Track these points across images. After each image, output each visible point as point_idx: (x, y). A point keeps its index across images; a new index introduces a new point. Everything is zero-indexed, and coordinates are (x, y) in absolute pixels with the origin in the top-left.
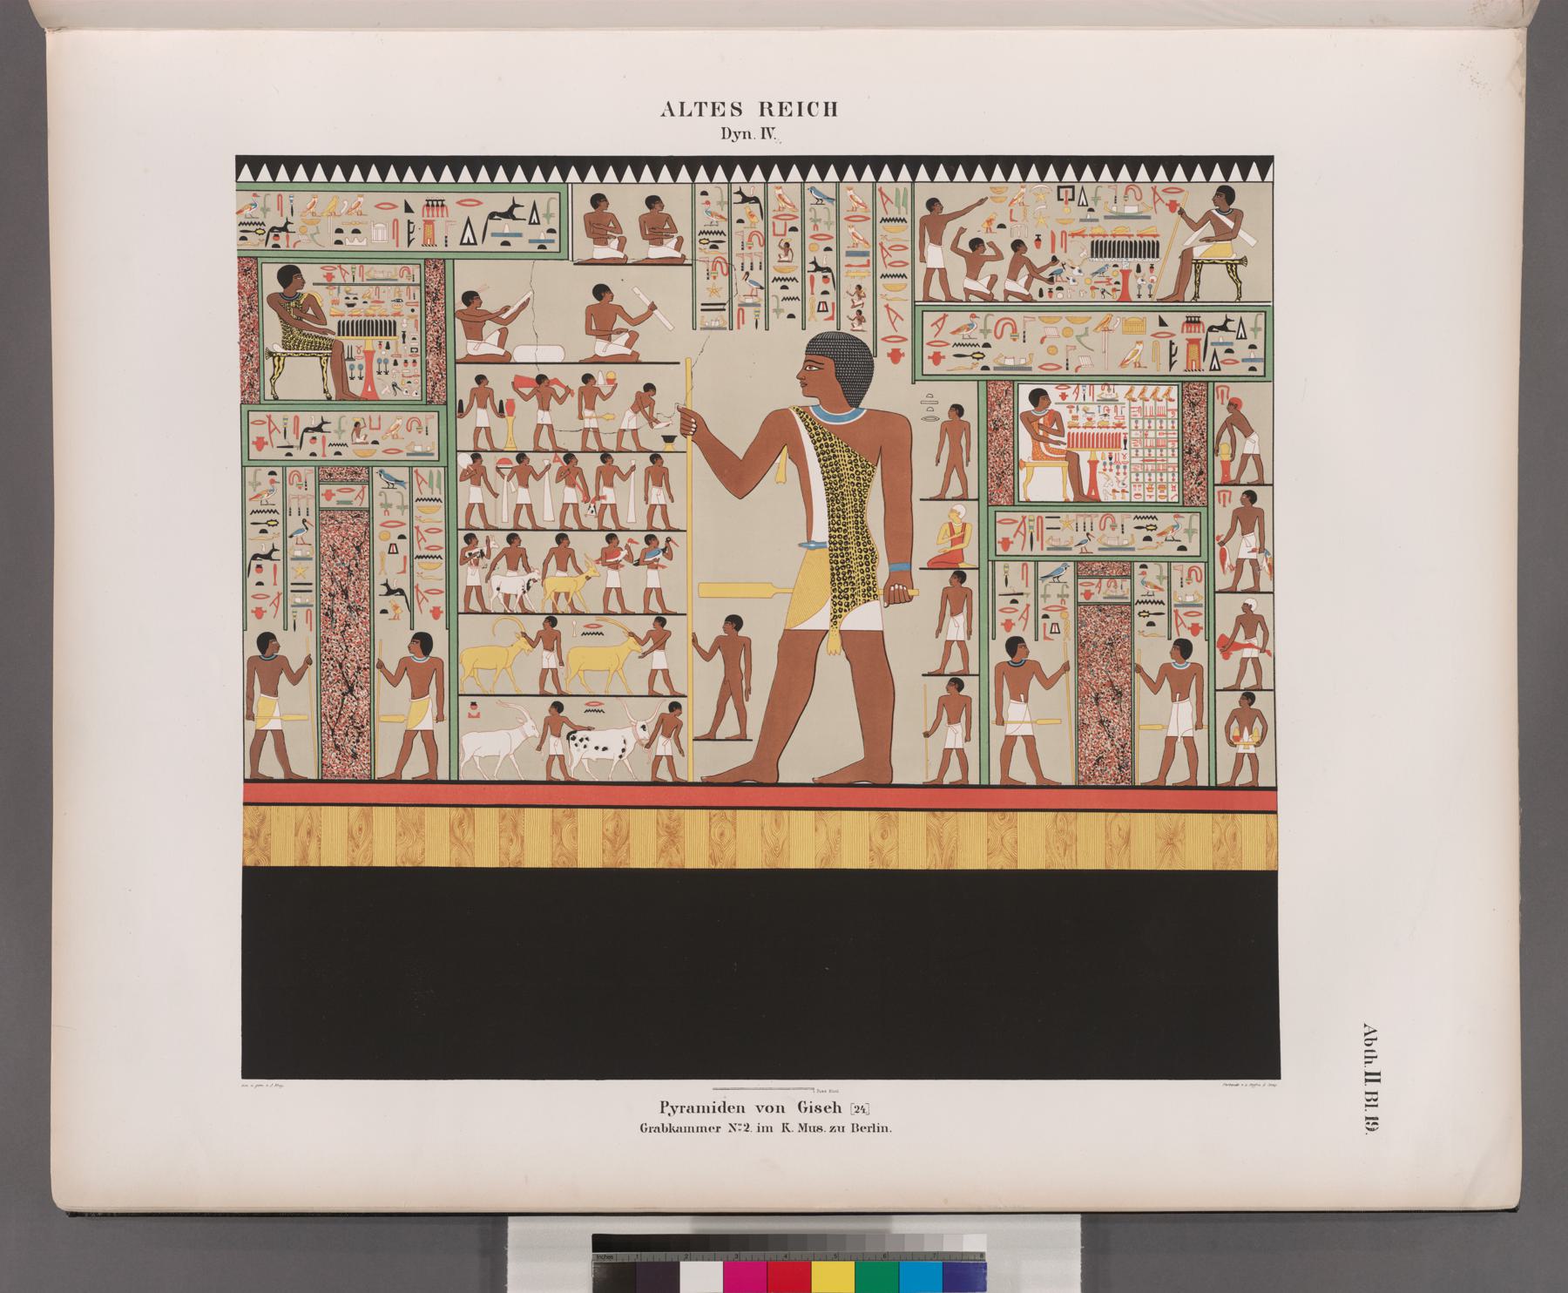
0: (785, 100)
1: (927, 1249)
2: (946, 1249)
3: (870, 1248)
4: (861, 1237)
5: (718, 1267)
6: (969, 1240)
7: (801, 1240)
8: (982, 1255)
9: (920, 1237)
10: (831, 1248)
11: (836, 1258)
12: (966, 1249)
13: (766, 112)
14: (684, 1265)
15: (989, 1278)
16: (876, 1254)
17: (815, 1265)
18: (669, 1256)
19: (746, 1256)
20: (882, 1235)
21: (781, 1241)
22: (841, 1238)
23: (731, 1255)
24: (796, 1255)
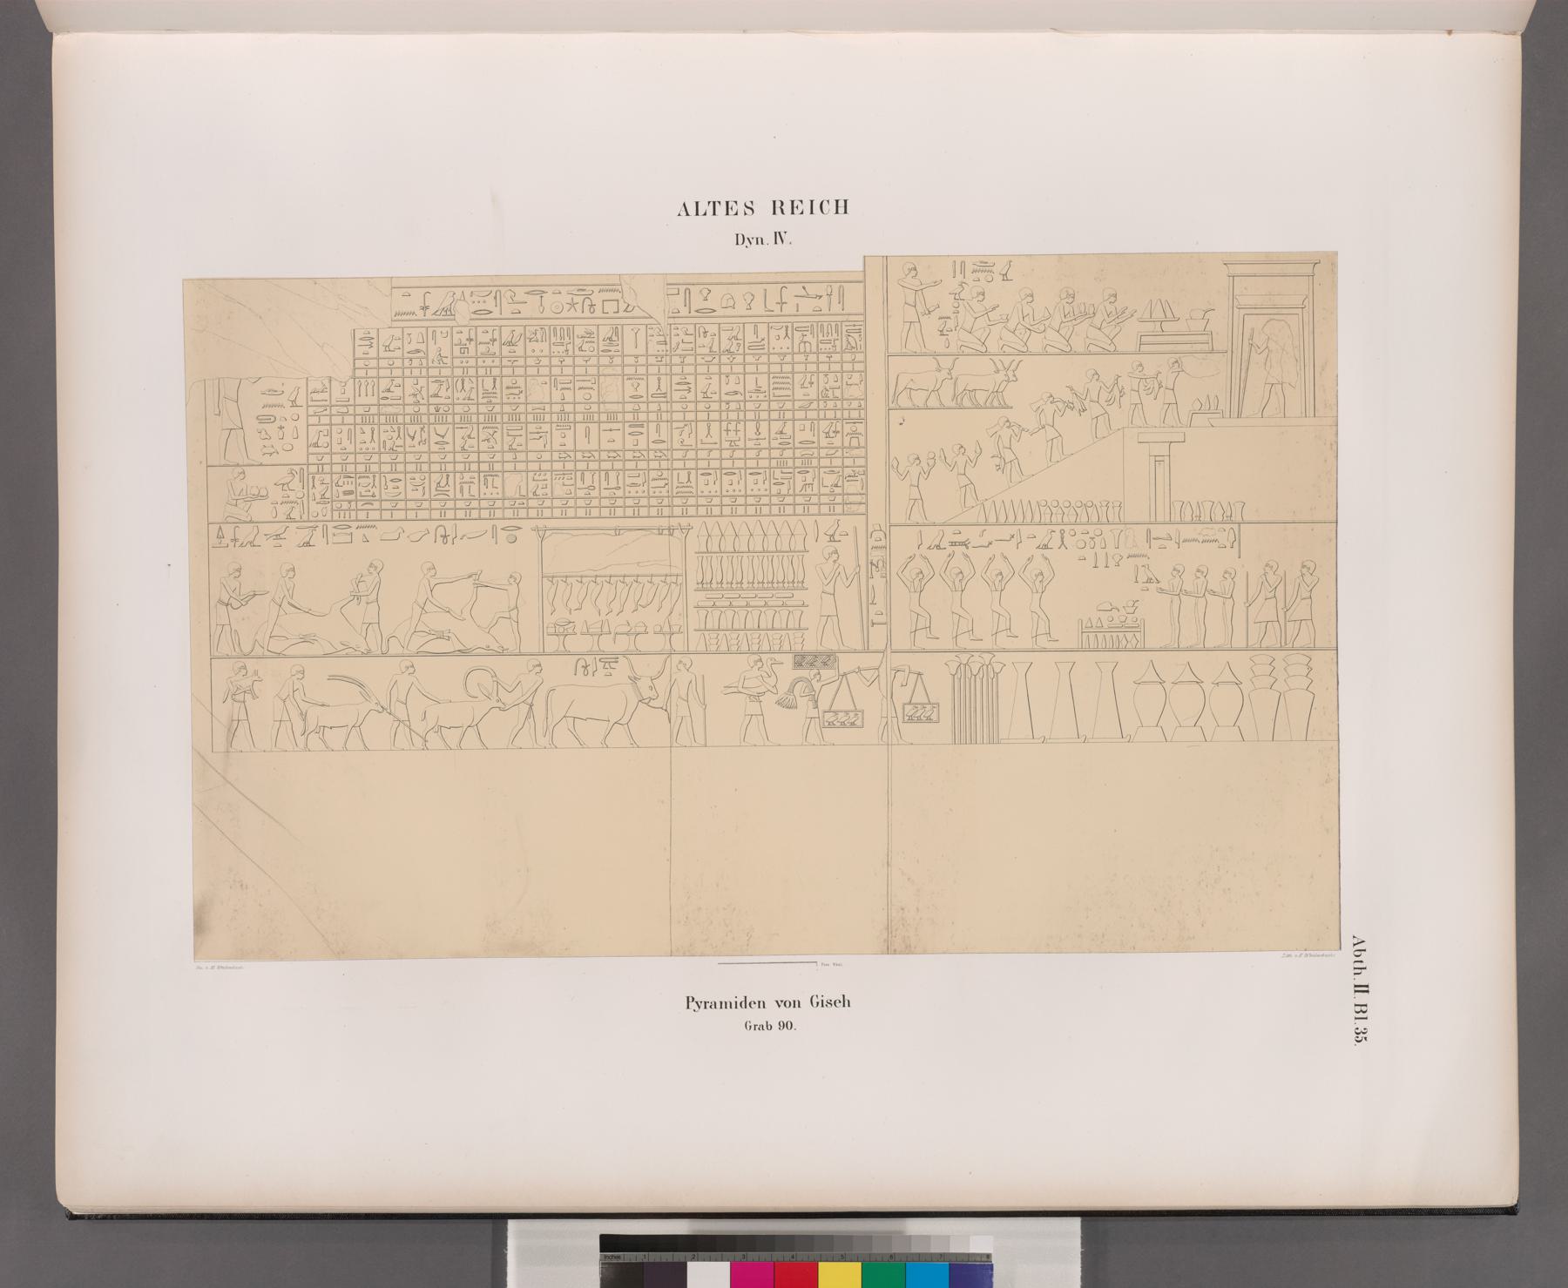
0: (796, 198)
3: (877, 1249)
4: (868, 1238)
5: (727, 1264)
6: (973, 1239)
7: (808, 1241)
9: (928, 1237)
10: (839, 1249)
11: (843, 1259)
13: (778, 210)
15: (995, 1280)
16: (882, 1255)
17: (823, 1267)
18: (678, 1256)
19: (753, 1256)
20: (888, 1237)
21: (789, 1241)
22: (848, 1239)
23: (738, 1256)
24: (802, 1256)
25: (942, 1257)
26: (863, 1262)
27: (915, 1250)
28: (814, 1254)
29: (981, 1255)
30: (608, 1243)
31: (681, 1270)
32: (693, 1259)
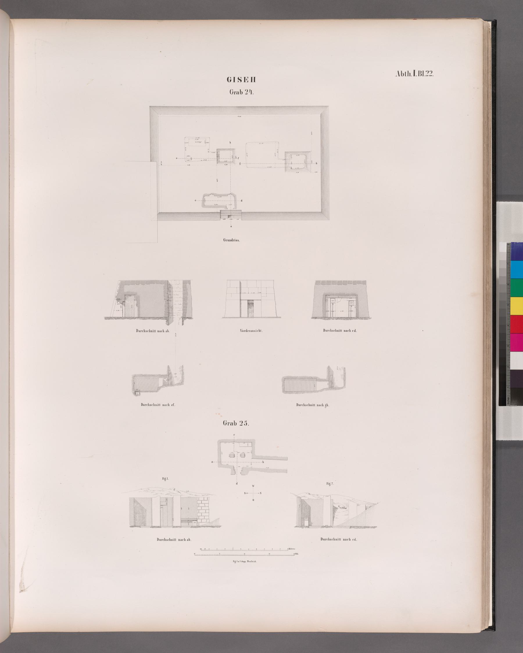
1: (506, 268)
2: (506, 259)
3: (505, 290)
5: (511, 353)
7: (502, 319)
8: (508, 244)
11: (509, 305)
12: (506, 251)
14: (513, 367)
15: (518, 242)
16: (508, 288)
18: (508, 374)
19: (508, 342)
21: (503, 327)
23: (508, 348)
24: (508, 322)
25: (508, 264)
26: (510, 296)
27: (505, 275)
28: (508, 317)
29: (507, 247)
30: (503, 403)
31: (513, 371)
32: (509, 367)
